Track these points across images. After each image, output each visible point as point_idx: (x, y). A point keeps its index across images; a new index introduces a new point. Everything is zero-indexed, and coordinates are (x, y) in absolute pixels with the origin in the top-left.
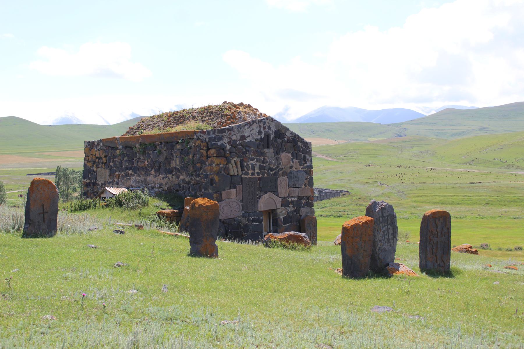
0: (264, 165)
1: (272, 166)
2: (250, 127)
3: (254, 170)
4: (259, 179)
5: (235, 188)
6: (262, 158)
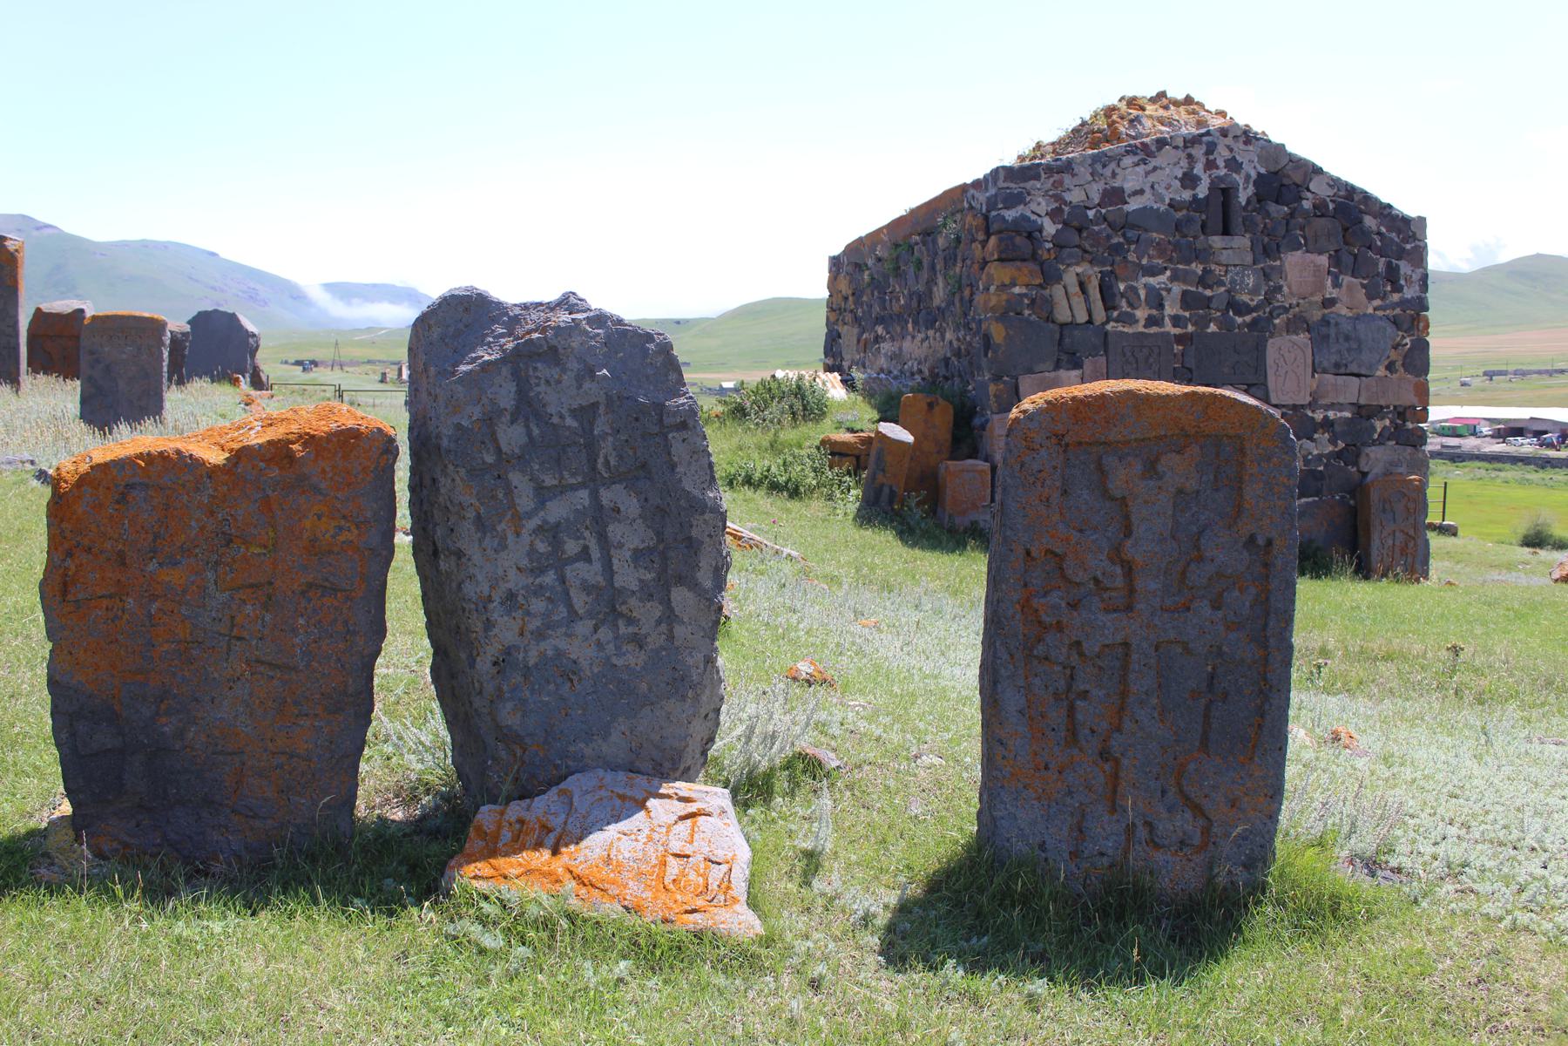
0: (1208, 293)
1: (1245, 298)
2: (1144, 162)
3: (1161, 306)
4: (1179, 339)
6: (1197, 268)
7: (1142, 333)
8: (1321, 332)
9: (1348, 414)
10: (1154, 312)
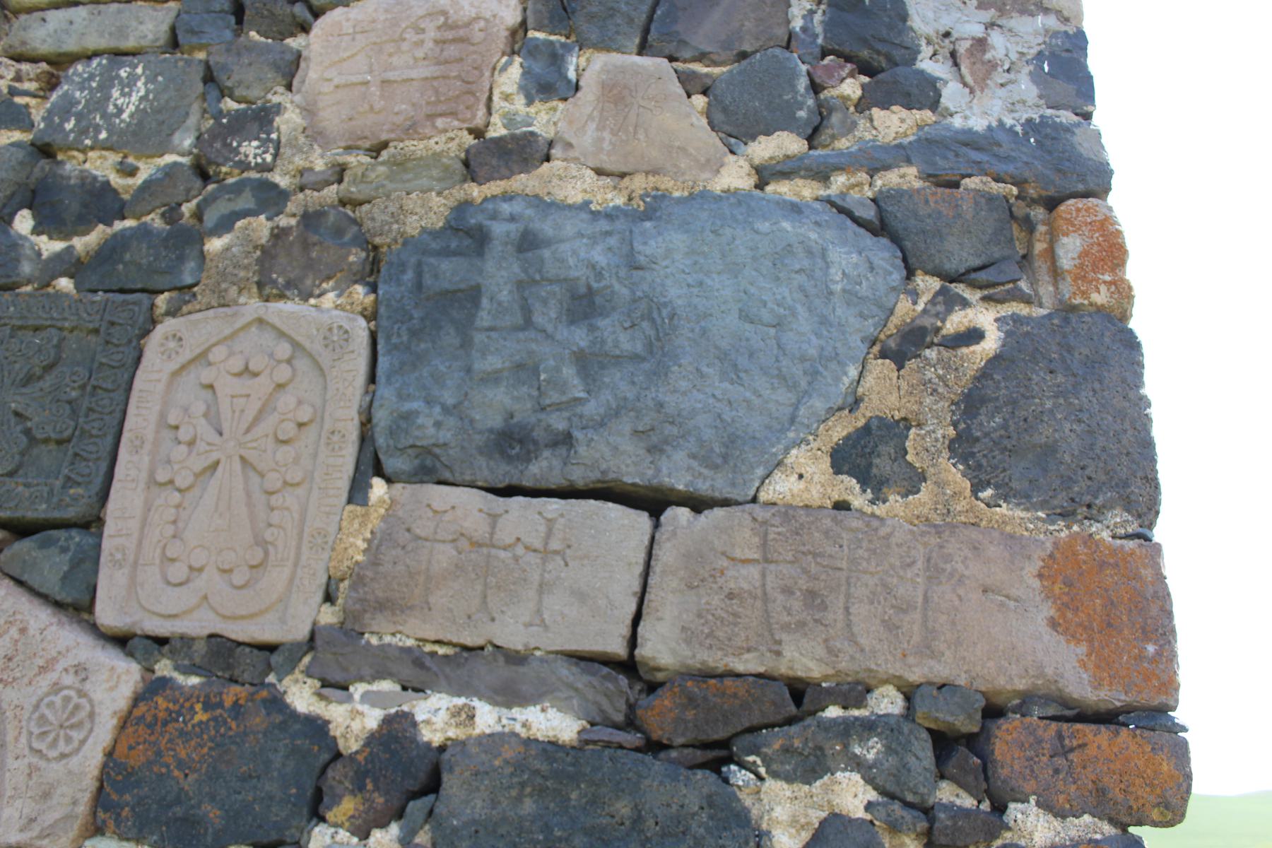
8: (424, 295)
9: (554, 723)
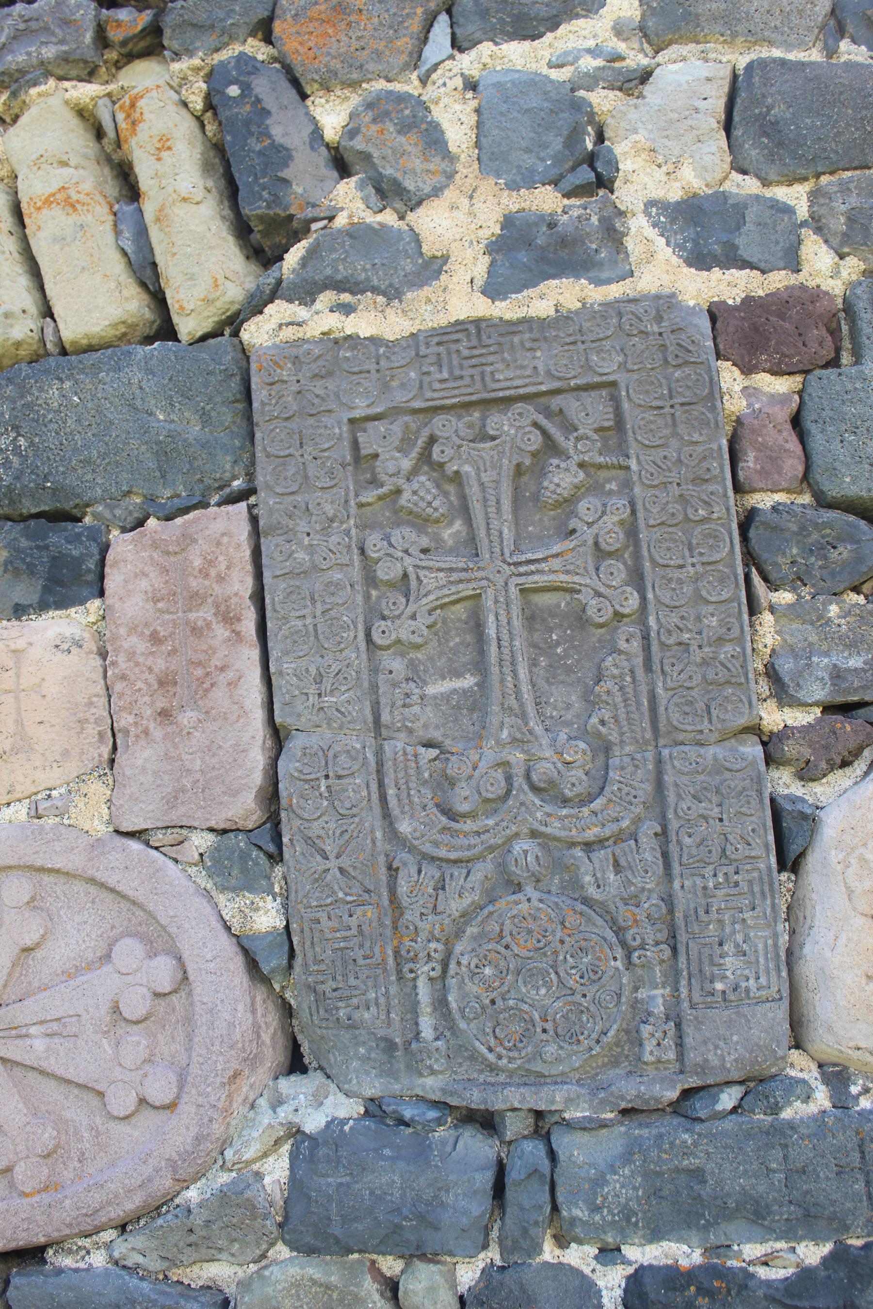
4: (747, 333)
5: (72, 580)
7: (477, 326)
10: (546, 200)
